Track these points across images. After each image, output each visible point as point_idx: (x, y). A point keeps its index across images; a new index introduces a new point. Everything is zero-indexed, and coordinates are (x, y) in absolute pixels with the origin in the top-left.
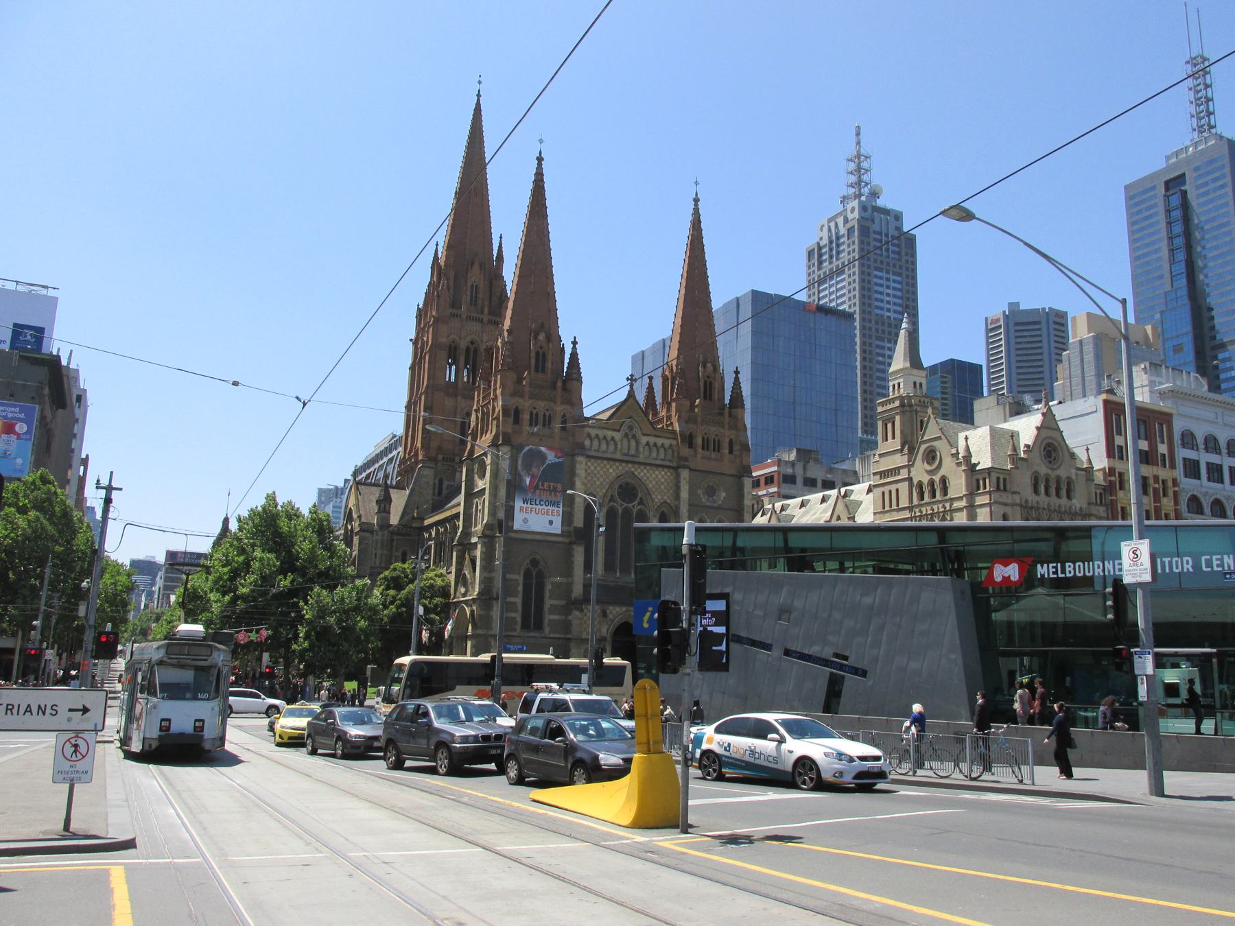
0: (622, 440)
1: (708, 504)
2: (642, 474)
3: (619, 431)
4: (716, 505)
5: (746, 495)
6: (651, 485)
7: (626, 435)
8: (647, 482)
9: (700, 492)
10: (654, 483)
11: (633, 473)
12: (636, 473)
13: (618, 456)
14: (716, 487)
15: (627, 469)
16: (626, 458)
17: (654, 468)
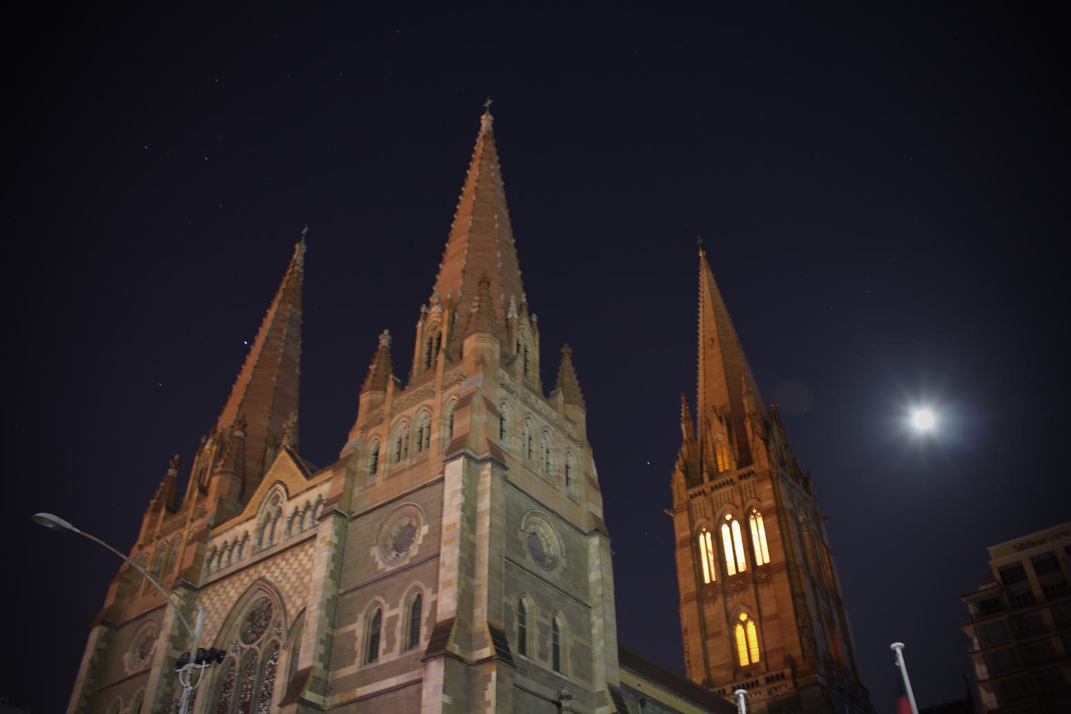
0: (261, 529)
1: (389, 569)
2: (277, 573)
3: (253, 517)
4: (407, 562)
5: (446, 503)
6: (288, 587)
7: (269, 515)
8: (283, 583)
9: (375, 551)
10: (293, 579)
11: (262, 579)
12: (268, 576)
13: (245, 563)
14: (414, 524)
15: (255, 577)
16: (257, 558)
17: (297, 550)
